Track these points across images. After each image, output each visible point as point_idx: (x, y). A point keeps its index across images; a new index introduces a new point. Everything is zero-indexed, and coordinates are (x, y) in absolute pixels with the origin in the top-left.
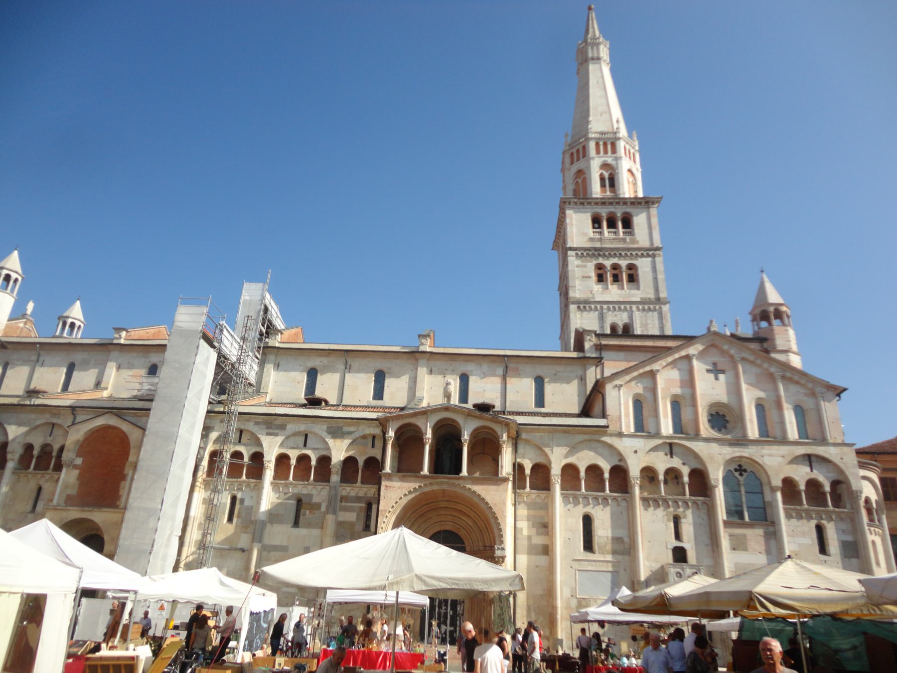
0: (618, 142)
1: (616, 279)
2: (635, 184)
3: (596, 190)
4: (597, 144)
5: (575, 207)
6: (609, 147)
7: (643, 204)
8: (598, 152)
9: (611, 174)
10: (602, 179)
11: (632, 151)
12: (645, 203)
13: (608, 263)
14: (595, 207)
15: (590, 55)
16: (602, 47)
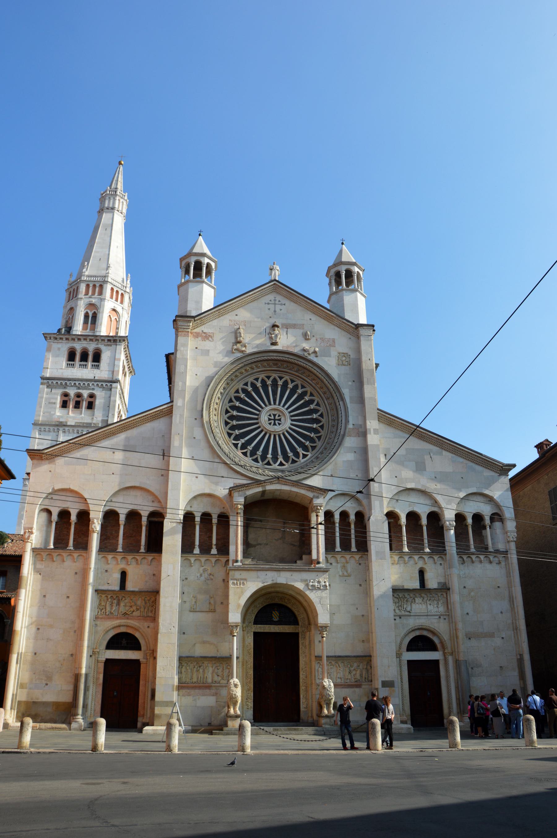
0: (105, 286)
1: (77, 405)
2: (118, 322)
3: (78, 328)
4: (88, 286)
5: (56, 341)
6: (97, 289)
7: (112, 342)
8: (87, 293)
9: (95, 312)
10: (86, 316)
11: (120, 292)
12: (114, 340)
13: (72, 392)
14: (72, 342)
15: (106, 205)
16: (117, 198)
